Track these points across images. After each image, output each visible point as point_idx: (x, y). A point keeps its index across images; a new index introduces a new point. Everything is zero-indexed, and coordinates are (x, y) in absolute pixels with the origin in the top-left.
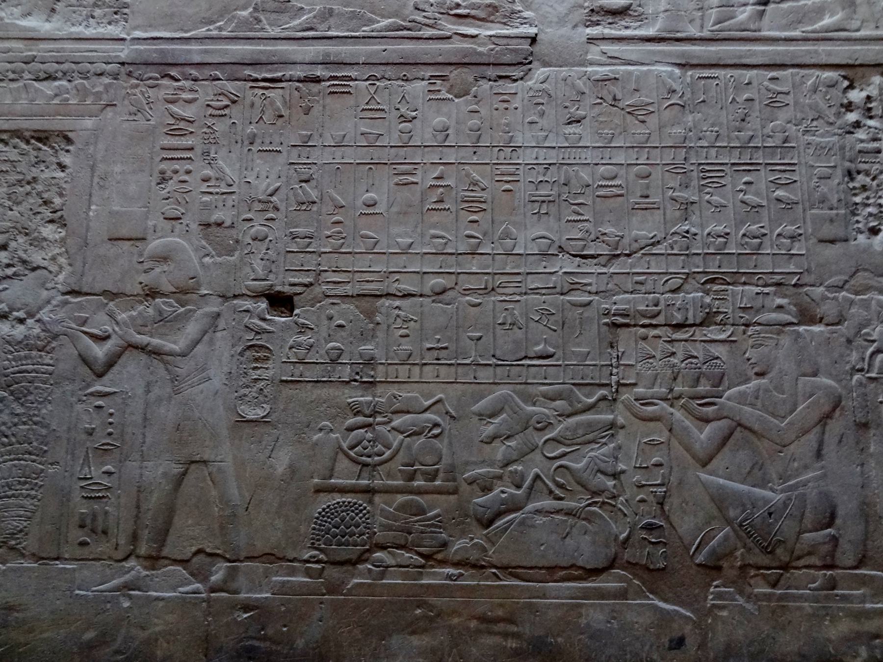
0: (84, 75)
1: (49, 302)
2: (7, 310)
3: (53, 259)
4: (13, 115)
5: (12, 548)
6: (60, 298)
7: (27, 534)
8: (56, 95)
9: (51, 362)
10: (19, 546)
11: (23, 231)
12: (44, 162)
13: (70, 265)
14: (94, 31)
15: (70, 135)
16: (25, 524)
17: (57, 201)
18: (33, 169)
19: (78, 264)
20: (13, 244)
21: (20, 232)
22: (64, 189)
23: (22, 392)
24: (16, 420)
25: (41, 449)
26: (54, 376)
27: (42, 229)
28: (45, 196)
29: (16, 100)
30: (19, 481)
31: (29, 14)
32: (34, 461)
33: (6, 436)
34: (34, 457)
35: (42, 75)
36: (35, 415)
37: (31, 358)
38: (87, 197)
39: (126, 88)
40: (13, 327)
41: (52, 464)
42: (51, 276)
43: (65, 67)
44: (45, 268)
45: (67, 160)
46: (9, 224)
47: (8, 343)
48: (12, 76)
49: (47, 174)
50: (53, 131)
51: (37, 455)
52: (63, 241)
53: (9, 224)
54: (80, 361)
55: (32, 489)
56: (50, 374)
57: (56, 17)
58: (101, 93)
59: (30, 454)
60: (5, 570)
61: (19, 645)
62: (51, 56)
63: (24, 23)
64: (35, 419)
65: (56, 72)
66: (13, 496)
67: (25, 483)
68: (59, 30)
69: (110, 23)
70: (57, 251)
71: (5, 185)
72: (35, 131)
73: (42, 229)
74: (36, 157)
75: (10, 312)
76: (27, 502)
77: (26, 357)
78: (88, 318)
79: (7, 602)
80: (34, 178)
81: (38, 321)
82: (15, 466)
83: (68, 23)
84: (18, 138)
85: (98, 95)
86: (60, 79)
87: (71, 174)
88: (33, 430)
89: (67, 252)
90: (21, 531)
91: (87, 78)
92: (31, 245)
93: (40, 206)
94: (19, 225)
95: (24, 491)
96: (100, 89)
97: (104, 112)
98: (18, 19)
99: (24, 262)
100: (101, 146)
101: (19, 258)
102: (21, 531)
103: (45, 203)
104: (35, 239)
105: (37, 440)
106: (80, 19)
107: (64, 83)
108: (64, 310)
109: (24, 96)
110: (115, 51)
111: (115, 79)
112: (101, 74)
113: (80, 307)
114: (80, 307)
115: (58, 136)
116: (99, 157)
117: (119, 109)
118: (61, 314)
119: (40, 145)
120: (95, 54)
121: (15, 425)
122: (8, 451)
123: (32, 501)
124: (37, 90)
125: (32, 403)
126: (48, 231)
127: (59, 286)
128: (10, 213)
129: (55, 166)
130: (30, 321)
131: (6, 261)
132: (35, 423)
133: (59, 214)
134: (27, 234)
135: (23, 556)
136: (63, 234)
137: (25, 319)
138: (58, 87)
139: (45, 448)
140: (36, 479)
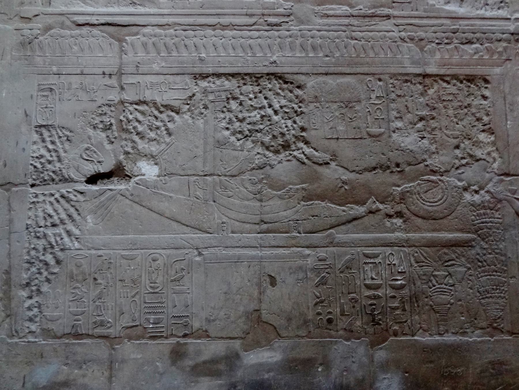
0: (490, 40)
1: (491, 180)
2: (466, 185)
3: (489, 154)
4: (452, 65)
5: (495, 328)
6: (497, 178)
7: (503, 320)
8: (475, 53)
9: (500, 216)
10: (499, 327)
11: (467, 137)
12: (473, 94)
13: (500, 157)
14: (491, 14)
15: (487, 78)
16: (501, 314)
17: (486, 119)
18: (467, 99)
19: (506, 156)
20: (462, 145)
21: (465, 138)
22: (489, 111)
23: (485, 235)
24: (485, 252)
25: (503, 269)
26: (502, 225)
27: (479, 136)
28: (478, 115)
29: (452, 56)
30: (493, 288)
31: (449, 2)
32: (500, 276)
33: (480, 262)
34: (499, 274)
35: (465, 41)
36: (496, 249)
37: (487, 214)
38: (504, 116)
39: (516, 49)
40: (473, 196)
41: (511, 278)
42: (489, 165)
43: (478, 35)
44: (484, 160)
45: (487, 93)
46: (458, 133)
47: (472, 205)
48: (446, 41)
49: (476, 102)
50: (477, 76)
51: (501, 273)
52: (494, 143)
53: (458, 133)
54: (515, 215)
55: (501, 293)
56: (501, 224)
57: (464, 5)
58: (502, 52)
59: (496, 272)
60: (494, 341)
61: (510, 385)
62: (468, 29)
63: (447, 7)
64: (496, 251)
65: (473, 38)
66: (491, 297)
67: (497, 289)
68: (469, 12)
69: (499, 8)
70: (490, 149)
71: (451, 109)
72: (466, 75)
73: (479, 136)
74: (468, 91)
75: (469, 187)
76: (500, 301)
77: (484, 214)
78: (516, 190)
79: (498, 360)
80: (469, 104)
81: (487, 192)
82: (488, 279)
83: (474, 8)
84: (456, 79)
85: (500, 54)
86: (475, 43)
87: (492, 102)
88: (496, 257)
89: (497, 149)
90: (499, 318)
91: (492, 43)
92: (473, 145)
93: (475, 121)
94: (464, 134)
95: (496, 294)
96: (500, 49)
97: (505, 63)
98: (442, 5)
99: (471, 156)
100: (507, 84)
101: (468, 153)
102: (499, 318)
103: (478, 120)
104: (476, 142)
105: (499, 263)
106: (481, 6)
107: (477, 45)
108: (501, 185)
109: (456, 53)
110: (505, 26)
111: (509, 43)
112: (500, 41)
113: (511, 183)
114: (511, 183)
115: (480, 78)
116: (507, 91)
117: (513, 62)
118: (500, 188)
119: (469, 84)
120: (495, 28)
121: (485, 255)
122: (483, 270)
123: (503, 300)
124: (463, 50)
125: (493, 241)
126: (482, 137)
127: (495, 170)
128: (457, 126)
129: (480, 97)
130: (482, 192)
131: (460, 156)
132: (497, 254)
133: (488, 126)
134: (470, 139)
135: (502, 332)
136: (493, 138)
137: (478, 191)
138: (476, 49)
139: (505, 268)
140: (502, 287)
